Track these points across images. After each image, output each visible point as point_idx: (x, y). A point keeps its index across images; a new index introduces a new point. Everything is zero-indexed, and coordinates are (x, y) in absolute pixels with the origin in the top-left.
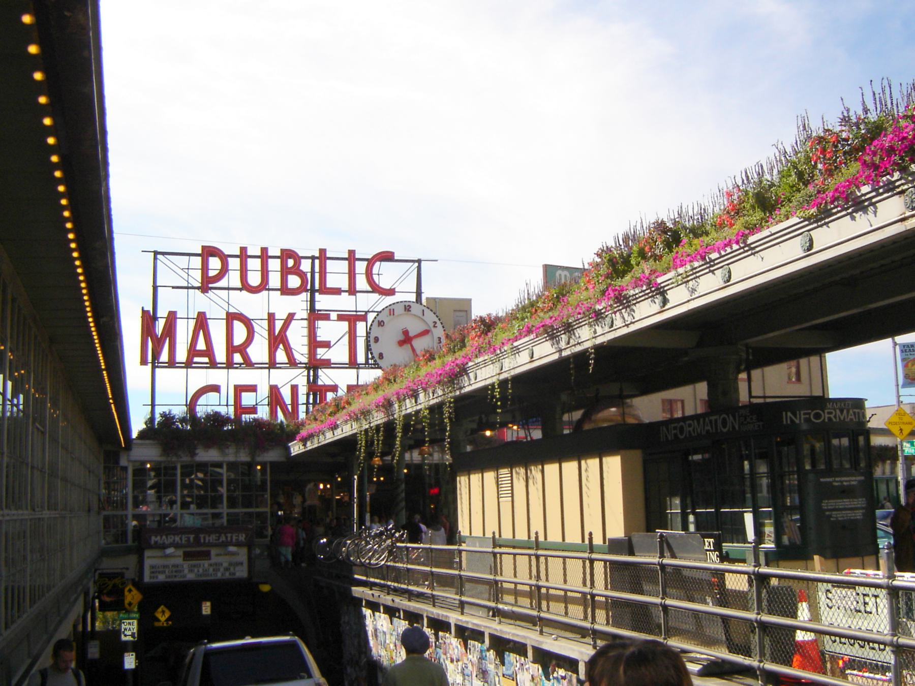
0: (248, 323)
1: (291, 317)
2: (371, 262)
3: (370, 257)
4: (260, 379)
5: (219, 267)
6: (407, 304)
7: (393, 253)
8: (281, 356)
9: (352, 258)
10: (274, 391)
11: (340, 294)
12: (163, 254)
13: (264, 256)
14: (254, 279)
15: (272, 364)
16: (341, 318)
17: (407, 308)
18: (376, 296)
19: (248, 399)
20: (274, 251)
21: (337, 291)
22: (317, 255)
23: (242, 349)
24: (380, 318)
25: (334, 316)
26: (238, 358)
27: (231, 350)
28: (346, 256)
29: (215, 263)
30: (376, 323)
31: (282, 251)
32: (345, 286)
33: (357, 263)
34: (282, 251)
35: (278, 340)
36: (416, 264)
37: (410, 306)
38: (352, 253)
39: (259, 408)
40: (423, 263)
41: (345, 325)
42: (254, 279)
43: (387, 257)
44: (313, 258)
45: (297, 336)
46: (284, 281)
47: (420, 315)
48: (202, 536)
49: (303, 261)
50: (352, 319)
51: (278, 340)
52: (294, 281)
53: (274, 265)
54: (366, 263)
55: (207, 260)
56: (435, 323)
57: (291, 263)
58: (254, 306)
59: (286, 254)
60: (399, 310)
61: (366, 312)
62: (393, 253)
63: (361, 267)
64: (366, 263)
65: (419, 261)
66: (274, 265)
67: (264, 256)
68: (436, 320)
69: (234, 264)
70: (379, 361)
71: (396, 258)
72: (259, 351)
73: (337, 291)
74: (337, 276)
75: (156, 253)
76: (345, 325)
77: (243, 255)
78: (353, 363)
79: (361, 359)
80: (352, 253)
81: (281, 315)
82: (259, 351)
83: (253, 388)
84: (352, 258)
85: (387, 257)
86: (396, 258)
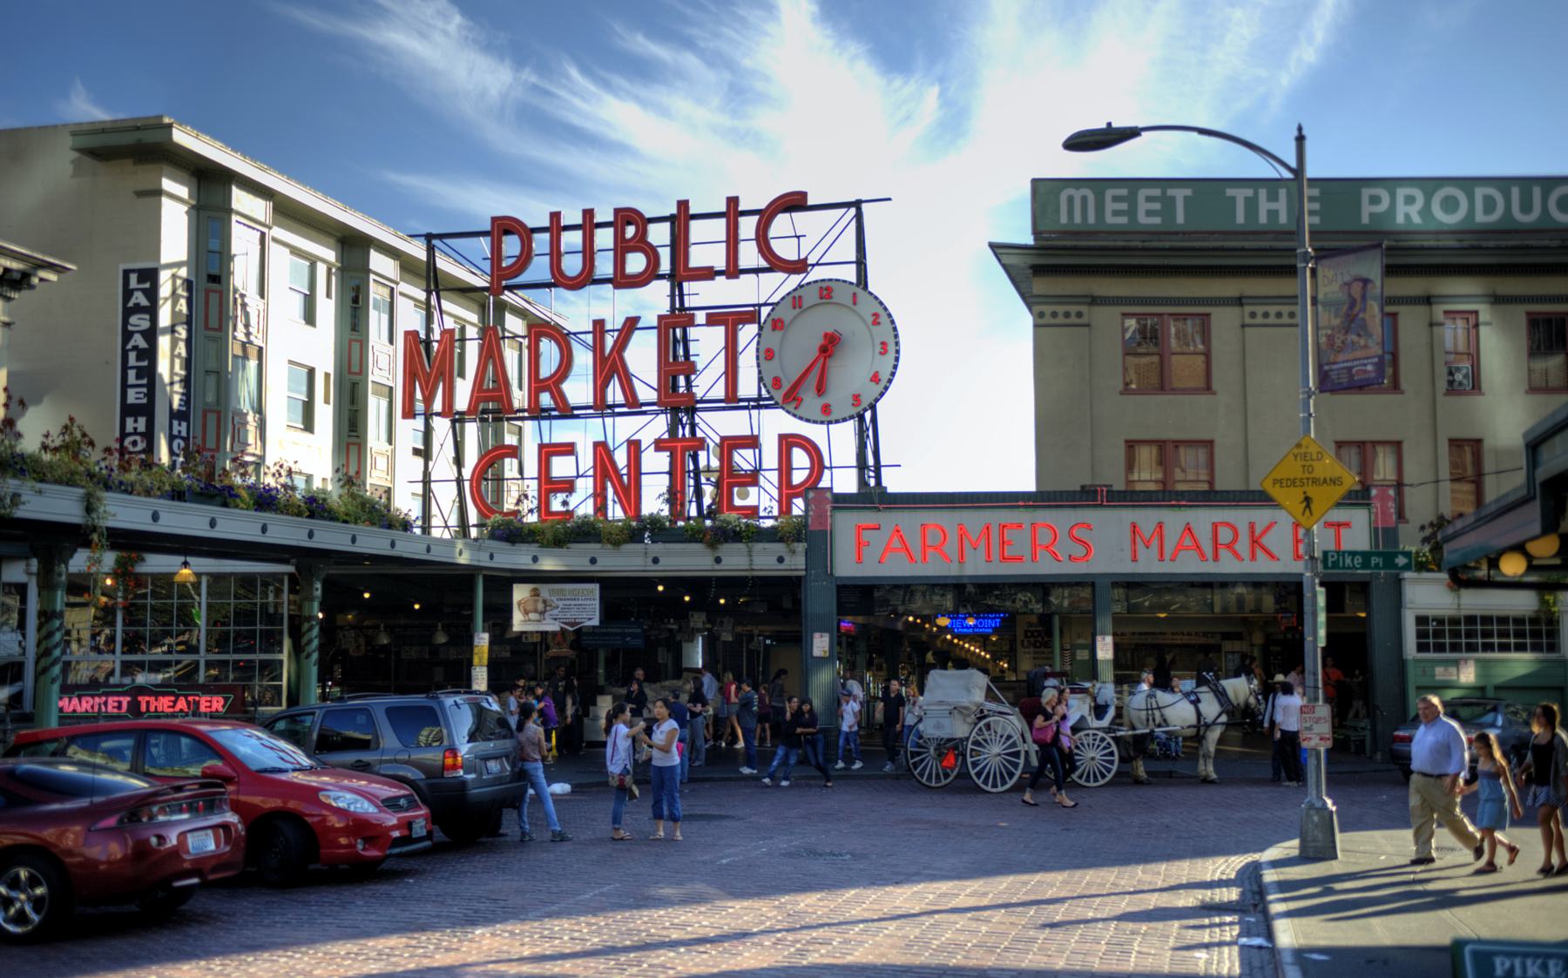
0: (563, 339)
1: (631, 324)
2: (766, 217)
3: (762, 206)
4: (583, 434)
5: (517, 251)
6: (824, 285)
7: (804, 195)
8: (615, 393)
9: (732, 212)
10: (602, 451)
11: (712, 278)
12: (441, 236)
13: (589, 224)
14: (572, 265)
15: (601, 407)
16: (712, 321)
17: (826, 290)
18: (781, 276)
19: (561, 467)
20: (604, 214)
21: (708, 274)
22: (674, 211)
23: (554, 384)
24: (775, 316)
25: (701, 317)
26: (546, 399)
27: (538, 385)
28: (723, 209)
29: (511, 246)
30: (769, 323)
31: (617, 211)
32: (720, 263)
33: (742, 220)
34: (617, 211)
35: (610, 366)
36: (853, 211)
37: (829, 289)
38: (733, 201)
39: (580, 483)
40: (864, 206)
41: (722, 329)
42: (572, 265)
43: (794, 203)
44: (671, 219)
45: (642, 357)
46: (620, 263)
47: (849, 302)
48: (143, 700)
49: (652, 227)
50: (729, 319)
51: (610, 366)
52: (636, 263)
53: (604, 238)
54: (756, 218)
55: (500, 242)
56: (876, 315)
57: (630, 231)
58: (575, 311)
59: (626, 216)
60: (811, 297)
61: (760, 305)
62: (804, 195)
63: (748, 226)
64: (756, 218)
65: (857, 204)
66: (604, 238)
67: (589, 224)
68: (880, 310)
69: (541, 242)
70: (774, 392)
71: (810, 202)
72: (578, 389)
73: (708, 274)
74: (706, 245)
75: (429, 237)
76: (722, 329)
77: (556, 226)
78: (732, 400)
79: (748, 386)
80: (733, 201)
81: (615, 322)
82: (578, 389)
83: (568, 449)
84: (732, 212)
85: (794, 203)
86: (810, 202)
